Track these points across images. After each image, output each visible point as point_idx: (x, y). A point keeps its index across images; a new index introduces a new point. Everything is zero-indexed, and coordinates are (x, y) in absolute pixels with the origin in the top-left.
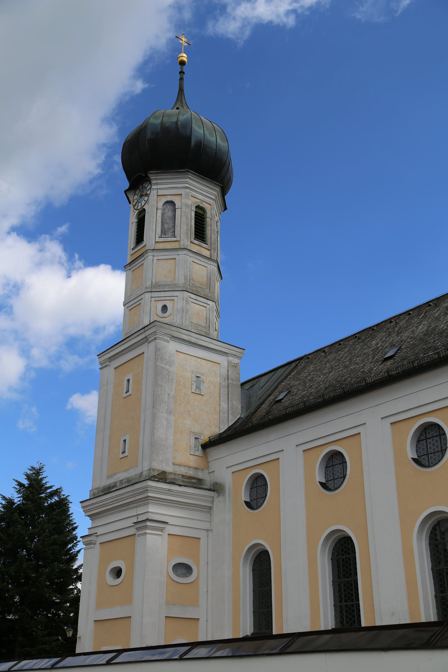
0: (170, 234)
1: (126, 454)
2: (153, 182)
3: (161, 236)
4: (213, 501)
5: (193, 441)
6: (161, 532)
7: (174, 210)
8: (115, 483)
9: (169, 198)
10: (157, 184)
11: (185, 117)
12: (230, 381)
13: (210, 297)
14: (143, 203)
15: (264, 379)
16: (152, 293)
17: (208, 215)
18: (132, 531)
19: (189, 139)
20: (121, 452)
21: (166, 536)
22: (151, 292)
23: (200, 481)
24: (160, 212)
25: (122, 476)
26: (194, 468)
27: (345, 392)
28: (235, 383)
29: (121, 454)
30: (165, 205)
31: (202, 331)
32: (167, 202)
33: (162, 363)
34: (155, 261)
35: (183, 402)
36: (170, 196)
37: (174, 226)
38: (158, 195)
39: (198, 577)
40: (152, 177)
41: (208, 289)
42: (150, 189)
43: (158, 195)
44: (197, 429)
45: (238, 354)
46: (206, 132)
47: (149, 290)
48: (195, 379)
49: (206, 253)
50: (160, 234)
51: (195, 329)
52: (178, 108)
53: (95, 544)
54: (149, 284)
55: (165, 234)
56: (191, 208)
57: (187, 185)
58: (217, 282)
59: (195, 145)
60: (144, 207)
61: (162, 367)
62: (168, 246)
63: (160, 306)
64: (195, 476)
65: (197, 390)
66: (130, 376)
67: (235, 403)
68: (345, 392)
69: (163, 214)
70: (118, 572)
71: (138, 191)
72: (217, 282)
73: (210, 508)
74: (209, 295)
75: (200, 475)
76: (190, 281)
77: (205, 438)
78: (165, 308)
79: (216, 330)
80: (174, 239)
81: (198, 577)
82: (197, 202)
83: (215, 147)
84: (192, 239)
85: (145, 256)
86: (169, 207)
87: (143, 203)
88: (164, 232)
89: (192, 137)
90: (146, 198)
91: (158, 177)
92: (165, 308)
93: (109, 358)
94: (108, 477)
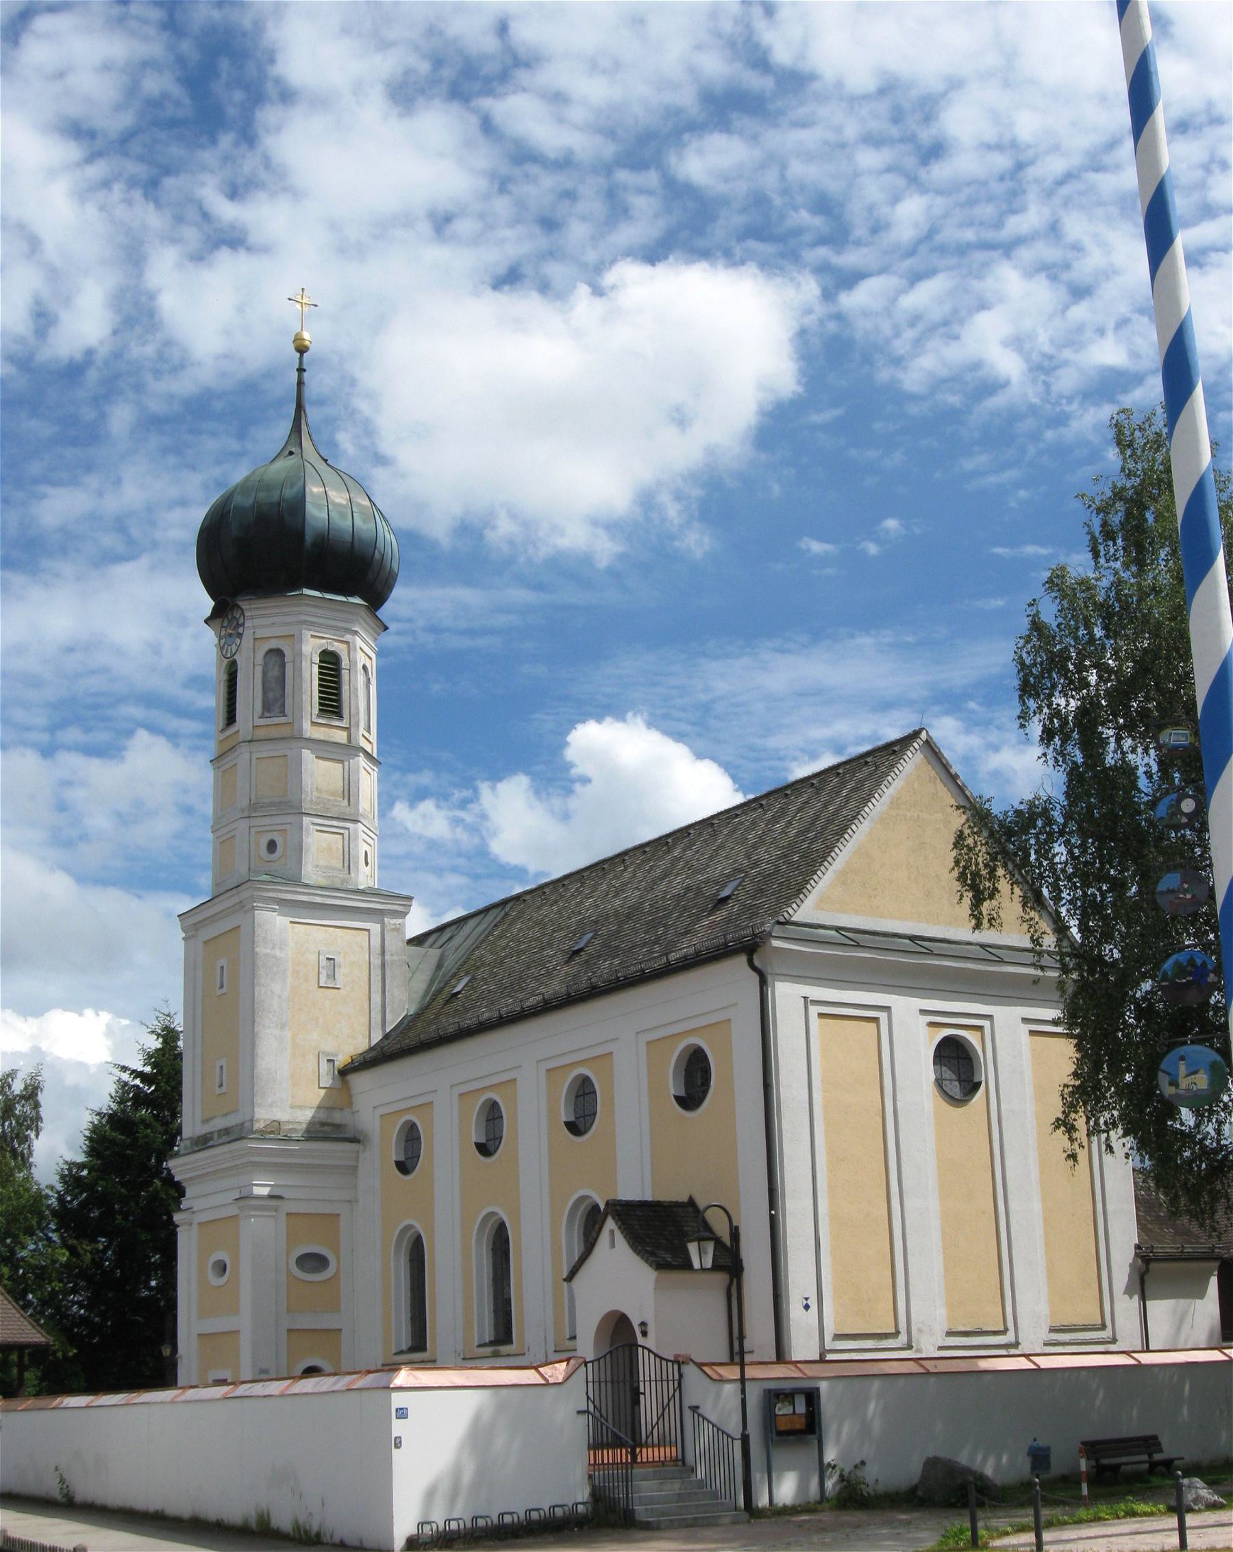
0: (277, 710)
1: (224, 1089)
2: (247, 614)
3: (263, 713)
4: (358, 1157)
5: (324, 1067)
6: (275, 1211)
7: (283, 666)
8: (211, 1133)
9: (273, 644)
10: (252, 618)
11: (295, 490)
12: (386, 958)
13: (351, 814)
14: (234, 647)
15: (472, 923)
16: (251, 819)
17: (345, 663)
18: (233, 1211)
19: (300, 534)
20: (217, 1084)
21: (283, 1218)
22: (249, 817)
23: (338, 1127)
24: (259, 670)
25: (219, 1123)
26: (327, 1108)
27: (501, 1017)
28: (395, 958)
29: (217, 1088)
30: (268, 656)
31: (336, 877)
32: (271, 651)
33: (265, 948)
34: (254, 761)
35: (305, 1005)
36: (276, 640)
37: (283, 695)
38: (255, 639)
39: (337, 1274)
40: (244, 605)
41: (346, 801)
42: (243, 625)
43: (255, 639)
44: (329, 1046)
45: (400, 909)
46: (334, 514)
47: (246, 814)
48: (324, 963)
49: (341, 737)
50: (260, 712)
51: (324, 877)
52: (291, 453)
53: (191, 1224)
54: (245, 803)
55: (269, 710)
56: (311, 660)
57: (304, 618)
58: (369, 774)
59: (314, 545)
60: (235, 657)
61: (266, 955)
62: (274, 733)
63: (264, 843)
64: (330, 1121)
65: (330, 981)
66: (223, 962)
67: (396, 993)
68: (501, 1017)
69: (265, 673)
70: (221, 1268)
71: (226, 621)
72: (369, 774)
73: (355, 1169)
74: (348, 810)
75: (337, 1117)
76: (312, 794)
77: (342, 1060)
78: (272, 846)
79: (367, 864)
80: (283, 720)
81: (337, 1274)
82: (323, 645)
83: (349, 538)
84: (314, 717)
85: (237, 753)
86: (274, 659)
87: (234, 647)
88: (268, 707)
89: (307, 531)
90: (238, 641)
91: (253, 606)
92: (272, 846)
93: (194, 924)
94: (206, 1121)
